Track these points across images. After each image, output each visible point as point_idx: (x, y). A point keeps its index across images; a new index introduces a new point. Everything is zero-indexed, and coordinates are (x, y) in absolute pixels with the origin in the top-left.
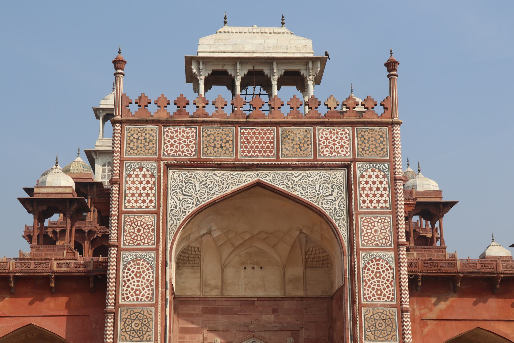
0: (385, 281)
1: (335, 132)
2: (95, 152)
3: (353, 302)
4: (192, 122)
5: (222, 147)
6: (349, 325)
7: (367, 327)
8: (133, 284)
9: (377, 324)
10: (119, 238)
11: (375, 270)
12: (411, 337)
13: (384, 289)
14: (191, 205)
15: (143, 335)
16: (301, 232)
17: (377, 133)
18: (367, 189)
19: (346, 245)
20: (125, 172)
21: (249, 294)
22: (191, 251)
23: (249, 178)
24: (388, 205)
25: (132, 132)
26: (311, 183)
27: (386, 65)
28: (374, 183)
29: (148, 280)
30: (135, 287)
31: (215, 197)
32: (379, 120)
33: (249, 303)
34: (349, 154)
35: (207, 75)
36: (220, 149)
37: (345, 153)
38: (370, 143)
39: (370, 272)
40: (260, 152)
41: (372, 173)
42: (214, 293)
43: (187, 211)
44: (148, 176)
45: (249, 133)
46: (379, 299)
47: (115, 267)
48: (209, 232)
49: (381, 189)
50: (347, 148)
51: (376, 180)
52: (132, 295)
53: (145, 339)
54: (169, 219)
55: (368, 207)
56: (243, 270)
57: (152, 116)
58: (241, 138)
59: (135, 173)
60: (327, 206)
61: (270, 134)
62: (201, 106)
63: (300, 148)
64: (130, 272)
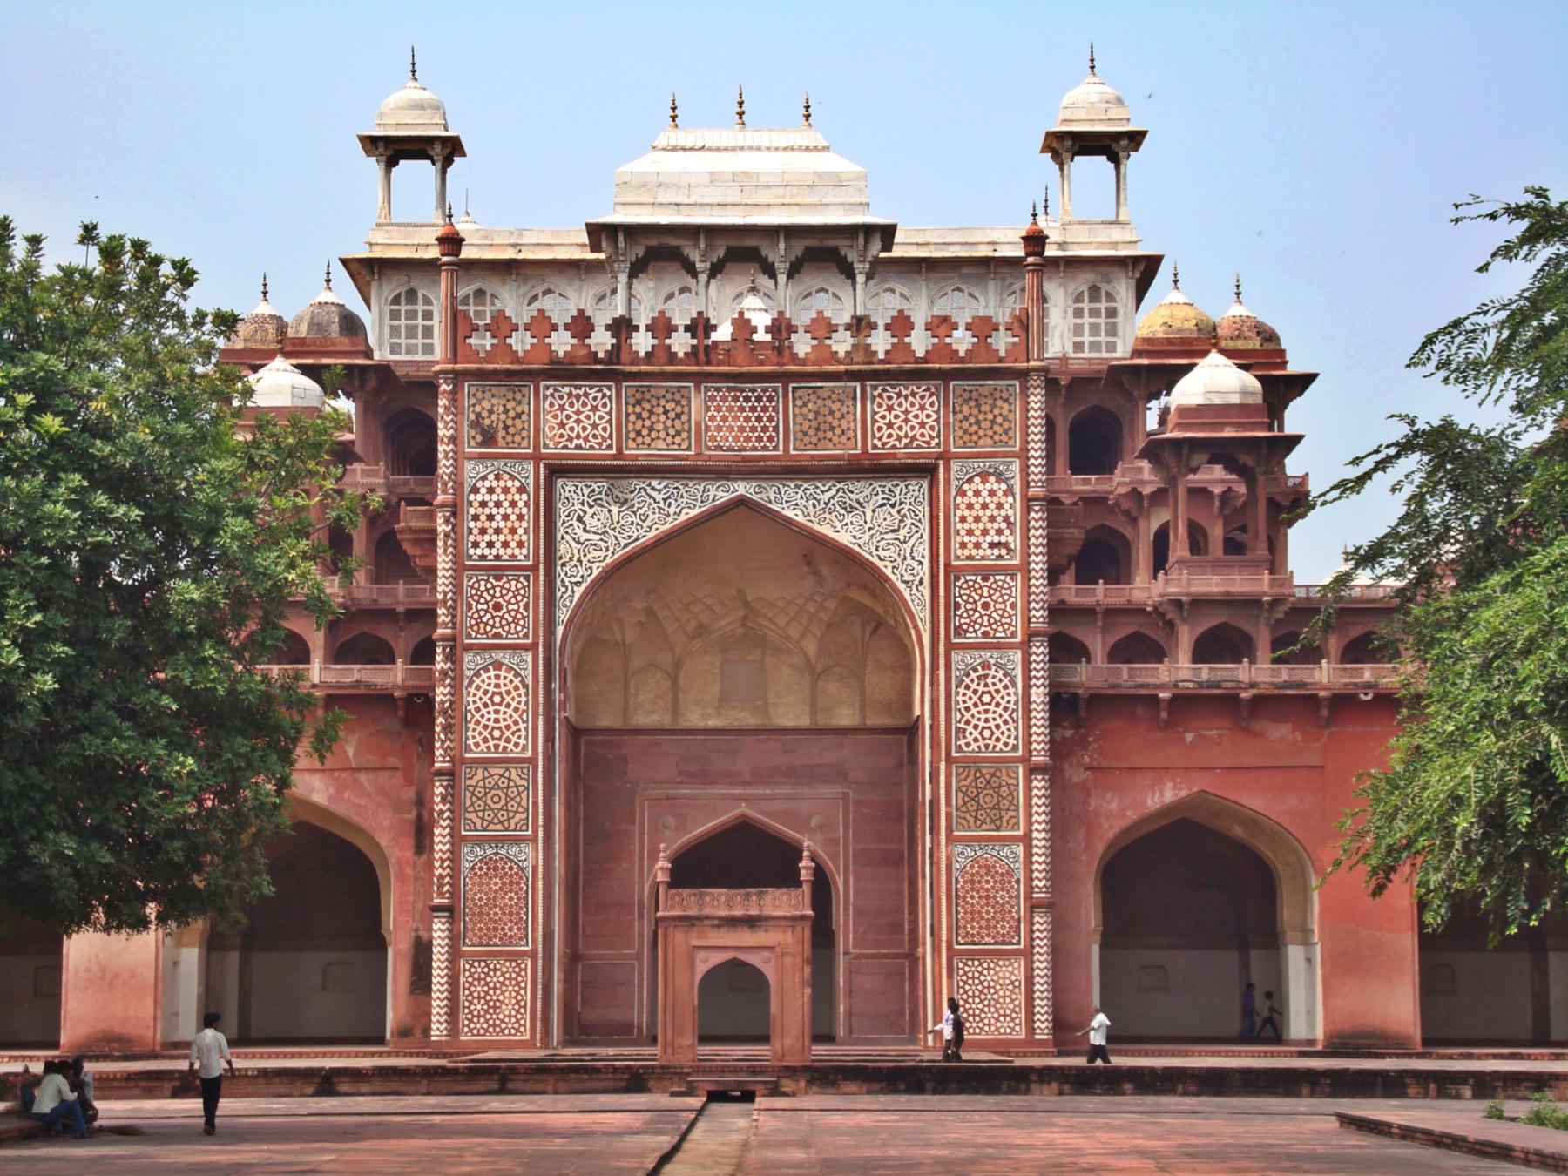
0: (1000, 710)
14: (603, 554)
26: (855, 504)
43: (594, 566)
44: (513, 490)
46: (987, 746)
50: (932, 428)
57: (518, 361)
60: (887, 553)
61: (770, 399)
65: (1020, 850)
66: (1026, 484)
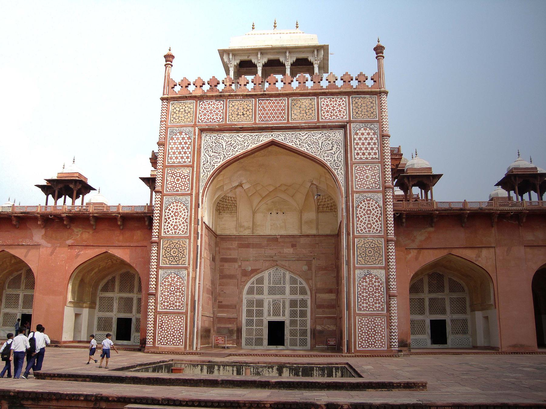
1: (334, 100)
3: (348, 234)
4: (221, 96)
5: (243, 114)
6: (344, 252)
7: (359, 253)
8: (172, 221)
9: (367, 251)
10: (162, 186)
11: (366, 208)
12: (394, 261)
13: (374, 223)
14: (219, 160)
15: (179, 260)
16: (312, 184)
17: (368, 100)
18: (360, 144)
19: (343, 189)
21: (274, 233)
22: (229, 200)
23: (265, 138)
24: (377, 156)
25: (175, 106)
26: (315, 140)
27: (375, 49)
28: (366, 139)
29: (183, 218)
30: (174, 224)
31: (238, 153)
32: (370, 90)
33: (273, 240)
34: (345, 116)
35: (236, 64)
36: (242, 116)
37: (342, 116)
38: (363, 108)
39: (362, 210)
40: (274, 117)
41: (364, 131)
42: (247, 232)
43: (216, 164)
44: (186, 138)
45: (265, 103)
46: (369, 231)
47: (159, 208)
48: (241, 185)
49: (372, 144)
50: (344, 112)
51: (367, 136)
52: (171, 230)
53: (180, 263)
54: (202, 171)
55: (361, 158)
56: (269, 215)
58: (259, 107)
59: (177, 136)
60: (328, 158)
62: (228, 84)
63: (306, 113)
64: (170, 212)
65: (383, 272)
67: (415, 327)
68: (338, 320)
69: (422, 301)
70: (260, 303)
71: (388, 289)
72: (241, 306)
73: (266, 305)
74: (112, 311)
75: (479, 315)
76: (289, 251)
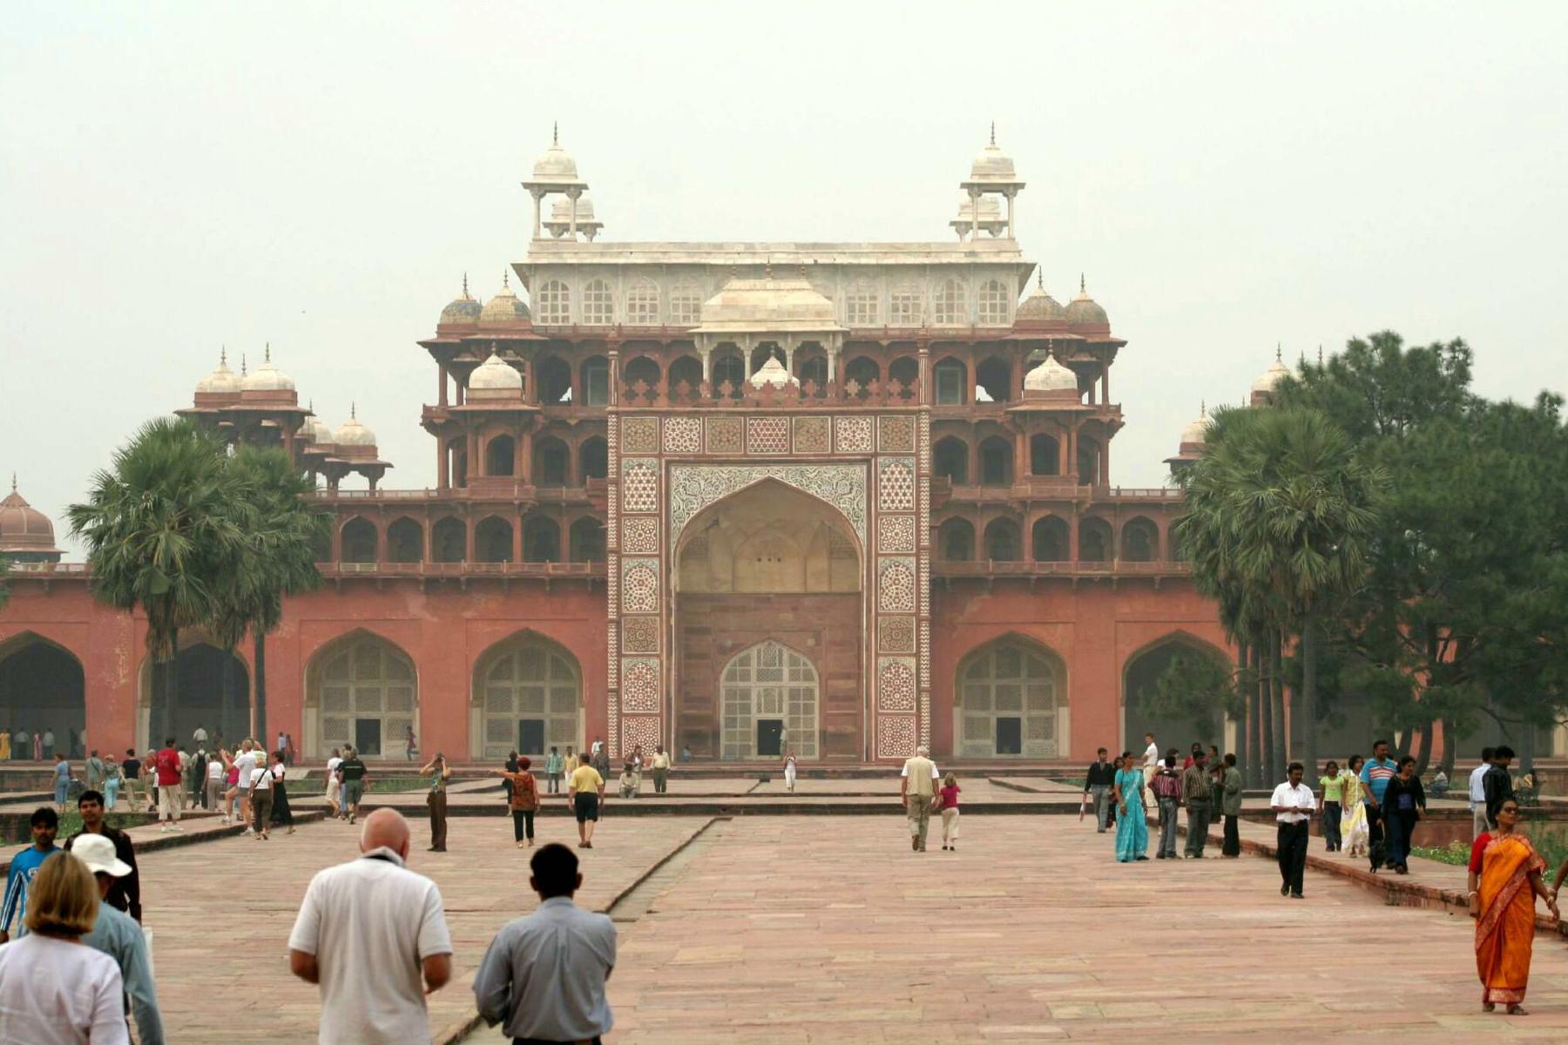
2: (529, 266)
3: (869, 611)
8: (636, 592)
20: (624, 470)
21: (764, 589)
23: (758, 474)
33: (764, 599)
42: (725, 589)
66: (918, 469)
67: (972, 728)
68: (856, 719)
69: (986, 690)
70: (746, 694)
71: (918, 682)
72: (718, 698)
73: (754, 696)
74: (509, 709)
75: (1064, 713)
76: (789, 616)
